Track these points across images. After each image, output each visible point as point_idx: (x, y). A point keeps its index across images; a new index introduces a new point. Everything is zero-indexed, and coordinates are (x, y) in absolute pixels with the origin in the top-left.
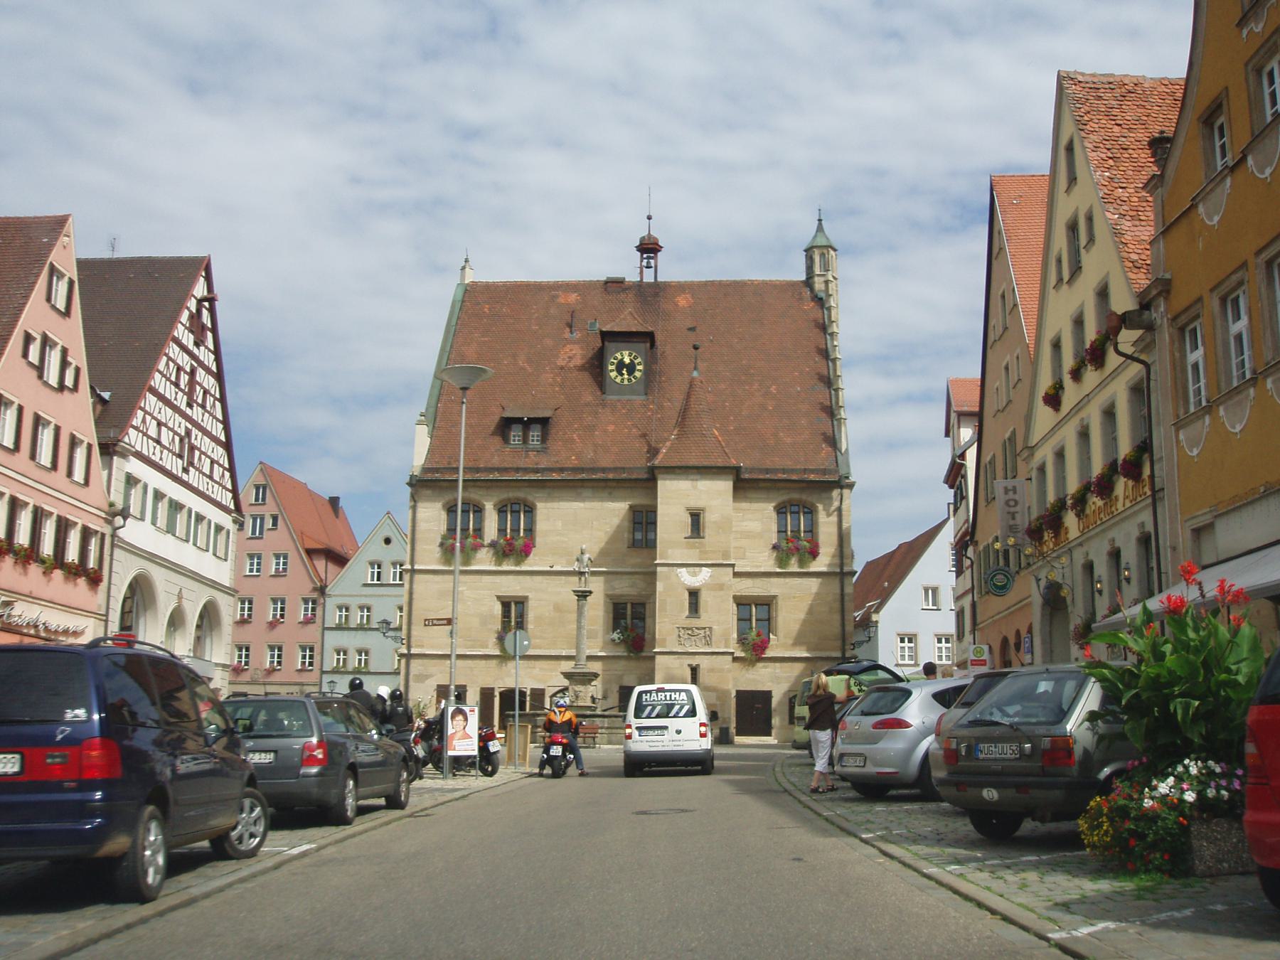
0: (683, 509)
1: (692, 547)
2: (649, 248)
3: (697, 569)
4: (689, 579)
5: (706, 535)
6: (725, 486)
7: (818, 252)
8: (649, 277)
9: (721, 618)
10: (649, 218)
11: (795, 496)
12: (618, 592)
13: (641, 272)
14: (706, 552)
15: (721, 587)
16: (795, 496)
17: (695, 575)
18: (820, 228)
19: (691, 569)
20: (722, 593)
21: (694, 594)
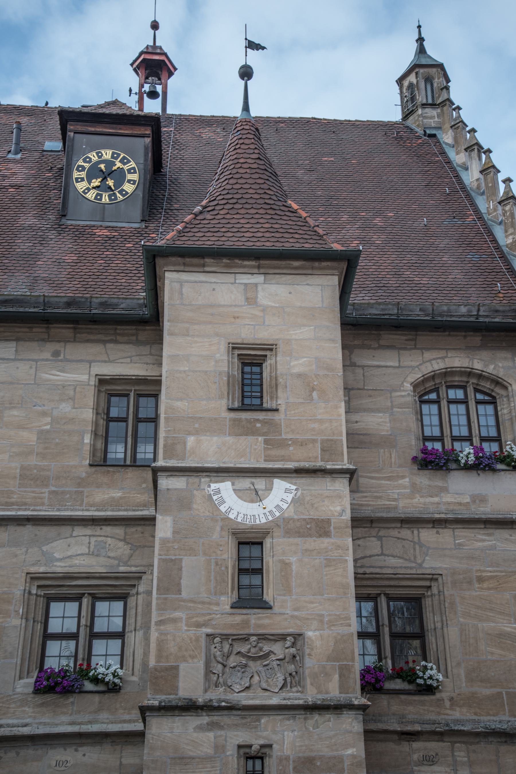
0: (223, 348)
1: (249, 430)
2: (154, 67)
3: (260, 483)
4: (232, 503)
5: (281, 402)
6: (315, 294)
7: (425, 80)
8: (152, 107)
9: (320, 609)
10: (155, 26)
11: (458, 361)
12: (60, 567)
13: (141, 102)
14: (283, 444)
15: (321, 528)
16: (458, 361)
17: (256, 497)
18: (421, 50)
19: (245, 483)
20: (325, 542)
21: (250, 543)
